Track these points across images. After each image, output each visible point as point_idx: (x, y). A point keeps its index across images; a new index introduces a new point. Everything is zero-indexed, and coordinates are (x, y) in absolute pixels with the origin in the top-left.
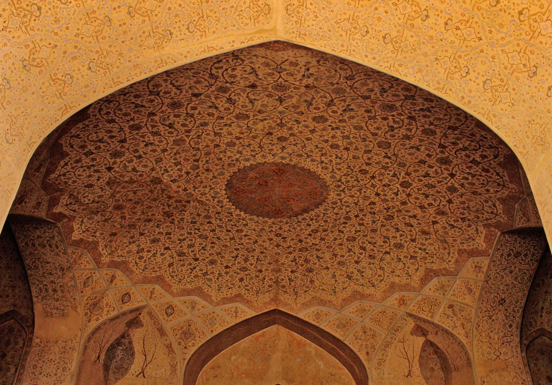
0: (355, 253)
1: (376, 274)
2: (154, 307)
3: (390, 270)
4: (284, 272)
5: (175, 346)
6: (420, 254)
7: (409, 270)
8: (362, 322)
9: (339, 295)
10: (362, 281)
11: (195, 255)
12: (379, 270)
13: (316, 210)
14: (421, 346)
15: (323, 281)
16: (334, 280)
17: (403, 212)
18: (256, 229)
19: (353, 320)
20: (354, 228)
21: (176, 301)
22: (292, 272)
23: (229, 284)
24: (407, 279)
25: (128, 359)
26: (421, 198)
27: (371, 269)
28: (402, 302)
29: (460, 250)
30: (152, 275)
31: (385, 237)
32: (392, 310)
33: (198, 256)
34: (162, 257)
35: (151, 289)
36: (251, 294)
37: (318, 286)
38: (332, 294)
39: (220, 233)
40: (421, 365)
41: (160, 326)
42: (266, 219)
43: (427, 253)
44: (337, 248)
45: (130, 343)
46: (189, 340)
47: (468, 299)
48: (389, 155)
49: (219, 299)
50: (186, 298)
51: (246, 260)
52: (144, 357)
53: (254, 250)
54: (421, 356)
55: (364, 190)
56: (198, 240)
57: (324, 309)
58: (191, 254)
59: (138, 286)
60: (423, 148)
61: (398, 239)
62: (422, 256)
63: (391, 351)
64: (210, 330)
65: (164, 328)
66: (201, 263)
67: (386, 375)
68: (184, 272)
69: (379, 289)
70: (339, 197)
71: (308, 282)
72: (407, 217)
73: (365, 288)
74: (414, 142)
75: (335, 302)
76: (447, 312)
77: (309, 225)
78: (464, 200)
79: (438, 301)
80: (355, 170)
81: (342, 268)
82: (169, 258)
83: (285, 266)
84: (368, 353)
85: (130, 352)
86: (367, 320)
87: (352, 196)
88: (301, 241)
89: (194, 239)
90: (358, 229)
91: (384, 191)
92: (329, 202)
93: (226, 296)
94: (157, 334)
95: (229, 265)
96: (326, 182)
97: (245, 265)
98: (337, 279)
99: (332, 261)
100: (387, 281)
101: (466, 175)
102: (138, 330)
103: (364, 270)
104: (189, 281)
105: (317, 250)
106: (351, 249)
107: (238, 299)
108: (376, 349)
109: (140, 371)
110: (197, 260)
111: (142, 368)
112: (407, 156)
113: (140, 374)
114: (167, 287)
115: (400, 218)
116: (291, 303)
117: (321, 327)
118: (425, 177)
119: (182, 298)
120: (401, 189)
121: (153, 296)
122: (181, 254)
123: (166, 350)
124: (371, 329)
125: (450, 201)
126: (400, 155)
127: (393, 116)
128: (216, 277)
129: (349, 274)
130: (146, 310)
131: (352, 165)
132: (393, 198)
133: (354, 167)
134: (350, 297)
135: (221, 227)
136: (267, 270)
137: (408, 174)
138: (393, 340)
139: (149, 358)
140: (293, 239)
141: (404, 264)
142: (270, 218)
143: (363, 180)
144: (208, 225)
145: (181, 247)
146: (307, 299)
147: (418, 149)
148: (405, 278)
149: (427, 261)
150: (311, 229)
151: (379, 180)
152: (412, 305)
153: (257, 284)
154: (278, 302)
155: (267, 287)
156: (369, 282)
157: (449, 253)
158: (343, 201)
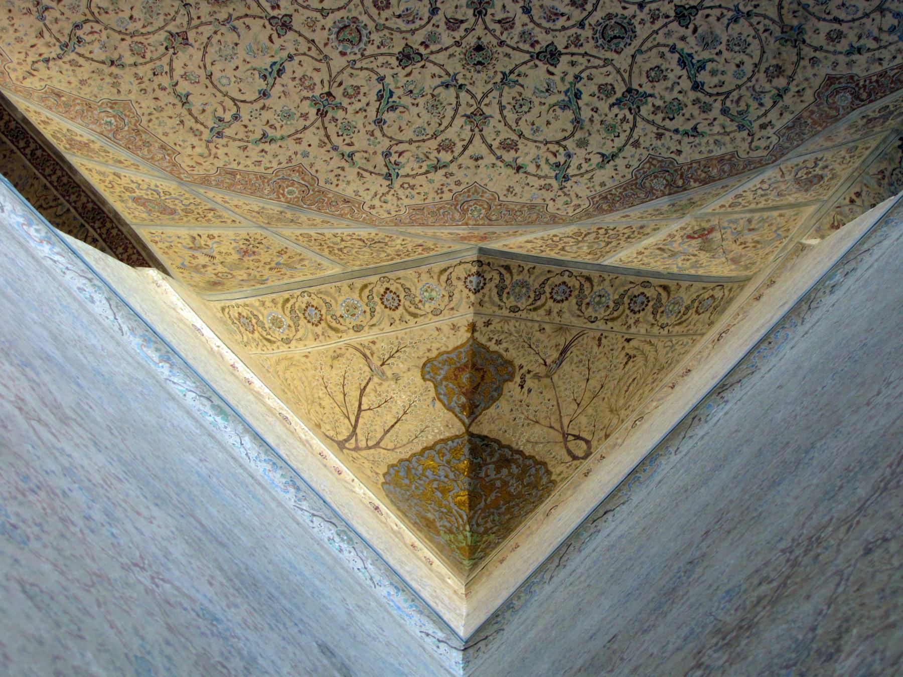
0: (434, 11)
1: (435, 136)
3: (506, 134)
7: (581, 153)
9: (221, 152)
10: (361, 141)
12: (459, 121)
15: (216, 70)
16: (261, 84)
24: (548, 187)
27: (435, 105)
29: (831, 80)
37: (179, 71)
43: (697, 86)
62: (669, 97)
69: (401, 192)
71: (163, 35)
73: (351, 173)
75: (185, 162)
81: (334, 55)
98: (276, 91)
100: (459, 175)
103: (407, 101)
129: (337, 92)
134: (263, 177)
138: (350, 322)
141: (577, 122)
146: (86, 92)
148: (542, 182)
149: (678, 123)
156: (387, 155)
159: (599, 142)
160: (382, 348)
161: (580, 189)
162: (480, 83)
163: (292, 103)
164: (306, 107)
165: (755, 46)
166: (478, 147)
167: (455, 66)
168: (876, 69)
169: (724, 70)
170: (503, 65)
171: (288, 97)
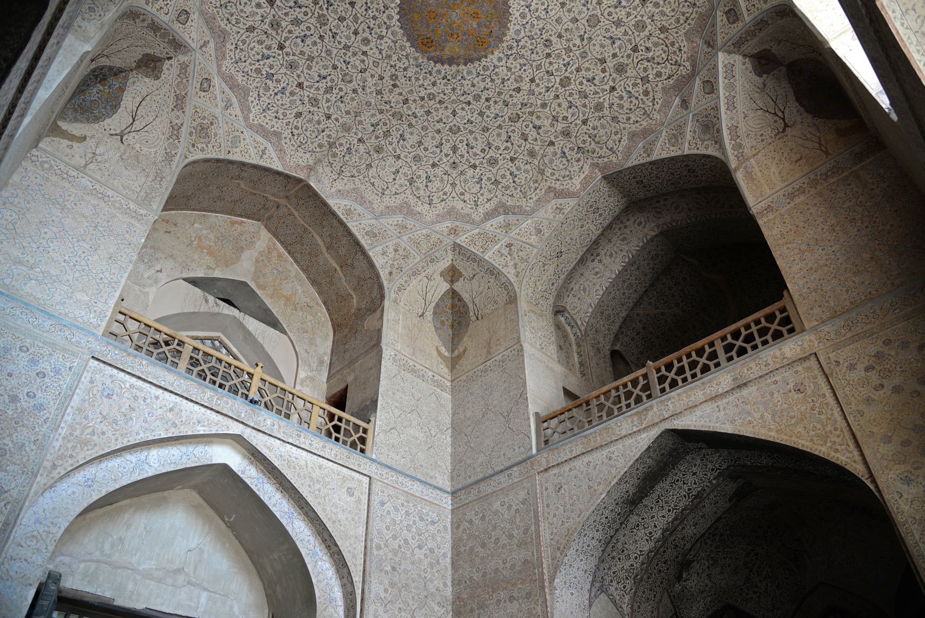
2: (197, 63)
4: (352, 134)
5: (184, 131)
10: (422, 192)
11: (287, 39)
13: (462, 67)
16: (393, 176)
18: (384, 52)
19: (389, 232)
20: (470, 115)
21: (216, 81)
22: (360, 140)
23: (281, 111)
25: (105, 108)
26: (564, 106)
27: (442, 180)
28: (454, 231)
30: (222, 23)
31: (489, 143)
32: (439, 236)
33: (287, 44)
34: (254, 9)
35: (207, 39)
36: (293, 142)
38: (377, 195)
39: (344, 29)
40: (435, 313)
41: (183, 93)
42: (408, 44)
43: (514, 182)
44: (430, 134)
45: (122, 90)
46: (202, 140)
47: (534, 239)
48: (586, 36)
49: (256, 122)
50: (227, 90)
51: (329, 90)
52: (131, 120)
53: (351, 81)
54: (437, 305)
55: (526, 68)
56: (313, 21)
57: (360, 209)
58: (284, 35)
59: (201, 21)
60: (618, 43)
61: (500, 152)
63: (414, 282)
64: (228, 149)
65: (188, 98)
66: (280, 57)
67: (402, 304)
68: (253, 52)
70: (496, 63)
72: (531, 125)
73: (420, 203)
74: (618, 32)
75: (375, 206)
76: (503, 251)
77: (434, 84)
78: (599, 125)
80: (544, 36)
82: (259, 18)
83: (360, 127)
84: (391, 273)
85: (113, 105)
86: (405, 238)
87: (509, 69)
88: (406, 101)
89: (310, 15)
90: (473, 119)
91: (542, 79)
92: (484, 63)
93: (264, 124)
94: (171, 102)
95: (306, 84)
96: (504, 34)
97: (320, 97)
99: (411, 150)
101: (624, 94)
102: (147, 80)
104: (246, 70)
105: (410, 125)
106: (442, 144)
107: (274, 140)
109: (118, 132)
110: (281, 47)
111: (122, 131)
112: (598, 46)
113: (116, 135)
114: (221, 56)
115: (525, 123)
116: (326, 182)
117: (349, 225)
118: (588, 81)
119: (224, 85)
121: (204, 49)
122: (276, 25)
123: (168, 131)
124: (405, 249)
125: (584, 122)
126: (594, 42)
128: (276, 90)
130: (183, 58)
131: (548, 27)
132: (540, 94)
133: (547, 31)
135: (356, 19)
136: (337, 120)
139: (137, 125)
140: (401, 94)
142: (412, 46)
143: (537, 53)
144: (348, 6)
145: (286, 14)
149: (508, 192)
150: (432, 91)
151: (551, 63)
153: (308, 133)
154: (313, 173)
155: (316, 144)
158: (497, 70)
159: (487, 195)
160: (431, 272)
161: (481, 210)
162: (454, 173)
163: (402, 181)
164: (406, 183)
166: (454, 194)
167: (447, 168)
168: (562, 187)
169: (522, 178)
171: (402, 180)
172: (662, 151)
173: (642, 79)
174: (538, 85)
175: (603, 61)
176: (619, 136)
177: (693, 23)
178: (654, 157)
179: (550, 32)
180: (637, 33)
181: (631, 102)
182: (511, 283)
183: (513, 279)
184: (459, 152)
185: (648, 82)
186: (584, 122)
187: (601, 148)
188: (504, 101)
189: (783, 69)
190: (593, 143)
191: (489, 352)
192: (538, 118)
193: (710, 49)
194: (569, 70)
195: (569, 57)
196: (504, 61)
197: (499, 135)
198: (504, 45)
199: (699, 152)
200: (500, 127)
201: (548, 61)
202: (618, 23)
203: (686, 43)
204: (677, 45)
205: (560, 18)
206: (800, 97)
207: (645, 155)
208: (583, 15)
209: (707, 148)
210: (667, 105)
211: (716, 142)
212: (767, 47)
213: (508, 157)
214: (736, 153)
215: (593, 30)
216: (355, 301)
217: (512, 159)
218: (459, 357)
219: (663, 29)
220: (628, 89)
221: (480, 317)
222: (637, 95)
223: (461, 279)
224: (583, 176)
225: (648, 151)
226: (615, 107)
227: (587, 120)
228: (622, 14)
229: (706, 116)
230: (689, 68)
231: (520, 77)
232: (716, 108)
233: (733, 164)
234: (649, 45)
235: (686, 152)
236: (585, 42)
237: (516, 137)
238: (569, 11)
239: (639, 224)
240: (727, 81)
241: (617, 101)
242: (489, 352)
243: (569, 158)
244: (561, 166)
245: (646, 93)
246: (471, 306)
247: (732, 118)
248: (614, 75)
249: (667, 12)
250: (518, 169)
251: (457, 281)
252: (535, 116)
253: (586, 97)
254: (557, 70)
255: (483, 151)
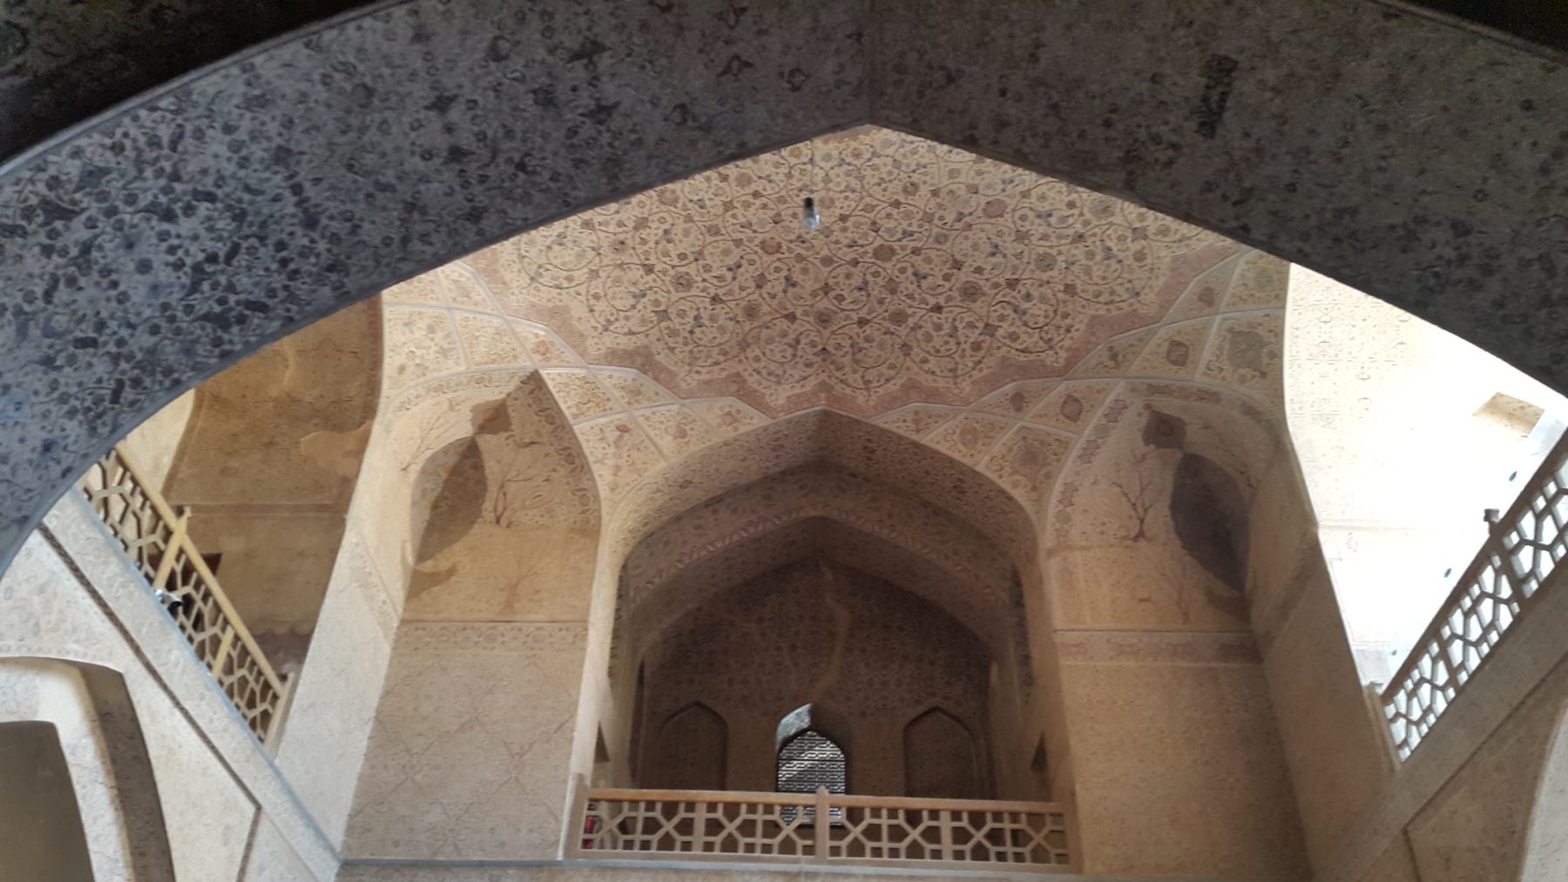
6: (683, 325)
8: (449, 309)
10: (533, 252)
14: (453, 439)
17: (799, 266)
27: (581, 255)
28: (543, 349)
29: (738, 375)
31: (701, 253)
43: (691, 332)
47: (667, 443)
48: (967, 219)
54: (433, 459)
60: (998, 259)
61: (706, 276)
70: (817, 159)
72: (784, 273)
79: (609, 405)
86: (458, 316)
87: (827, 179)
108: (429, 376)
115: (778, 264)
118: (915, 274)
120: (870, 249)
125: (862, 322)
126: (970, 234)
127: (1081, 214)
131: (932, 169)
132: (837, 242)
133: (925, 174)
137: (916, 251)
141: (634, 307)
147: (993, 254)
149: (671, 341)
151: (889, 216)
152: (558, 370)
157: (716, 364)
158: (809, 167)
159: (634, 324)
162: (609, 258)
165: (727, 337)
168: (755, 386)
169: (707, 334)
170: (625, 258)
172: (941, 438)
173: (987, 325)
174: (844, 230)
175: (958, 265)
176: (893, 373)
177: (1115, 313)
178: (927, 439)
179: (927, 178)
180: (1032, 267)
181: (947, 343)
182: (597, 498)
183: (604, 492)
184: (644, 233)
185: (992, 335)
186: (862, 322)
187: (855, 372)
188: (778, 215)
189: (1179, 455)
190: (849, 357)
191: (509, 605)
192: (805, 271)
193: (1111, 364)
194: (904, 242)
195: (920, 226)
196: (830, 164)
197: (726, 252)
198: (854, 144)
199: (999, 482)
200: (738, 243)
201: (889, 210)
202: (1022, 236)
203: (1082, 327)
204: (1068, 321)
205: (958, 171)
206: (1178, 506)
207: (913, 426)
208: (990, 192)
209: (1015, 486)
210: (993, 382)
211: (1034, 488)
212: (1185, 417)
213: (712, 291)
214: (1058, 525)
215: (983, 220)
216: (288, 374)
217: (715, 299)
218: (436, 579)
219: (1070, 289)
220: (957, 323)
221: (504, 522)
222: (962, 339)
223: (503, 435)
224: (797, 391)
225: (919, 422)
226: (920, 333)
227: (868, 321)
228: (1038, 228)
229: (1042, 443)
230: (1061, 361)
231: (832, 201)
232: (1065, 445)
233: (1047, 540)
234: (1035, 293)
235: (980, 468)
236: (959, 225)
237: (747, 274)
238: (979, 173)
239: (801, 488)
240: (1104, 421)
241: (929, 327)
242: (509, 605)
243: (800, 353)
244: (778, 357)
245: (976, 347)
246: (493, 490)
247: (1077, 473)
248: (955, 294)
249: (1097, 272)
250: (713, 319)
251: (494, 432)
252: (802, 265)
253: (893, 292)
254: (888, 230)
255: (682, 256)
